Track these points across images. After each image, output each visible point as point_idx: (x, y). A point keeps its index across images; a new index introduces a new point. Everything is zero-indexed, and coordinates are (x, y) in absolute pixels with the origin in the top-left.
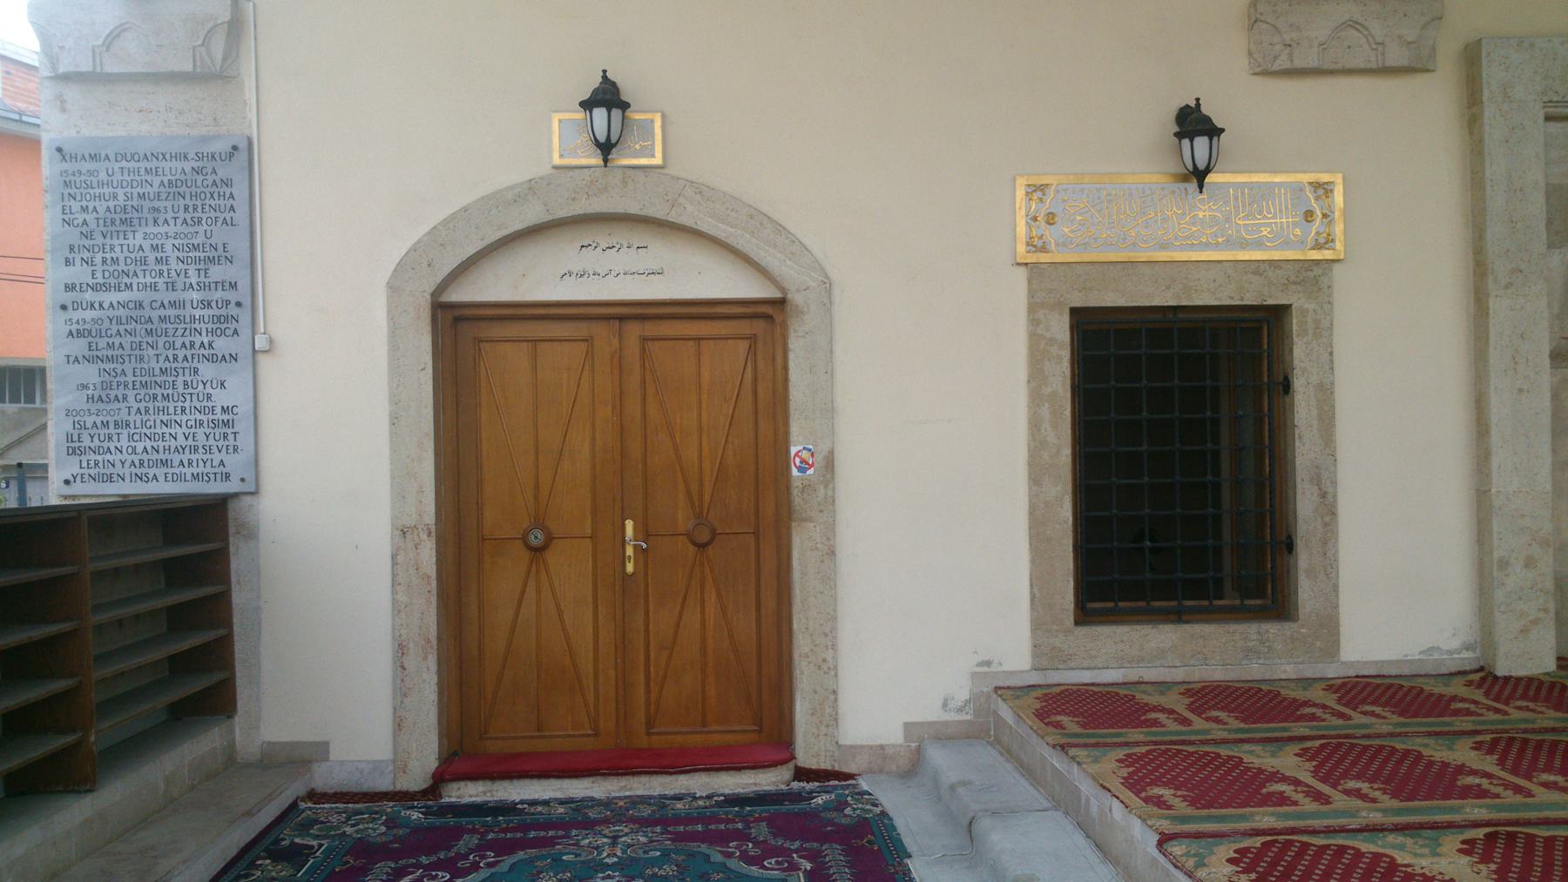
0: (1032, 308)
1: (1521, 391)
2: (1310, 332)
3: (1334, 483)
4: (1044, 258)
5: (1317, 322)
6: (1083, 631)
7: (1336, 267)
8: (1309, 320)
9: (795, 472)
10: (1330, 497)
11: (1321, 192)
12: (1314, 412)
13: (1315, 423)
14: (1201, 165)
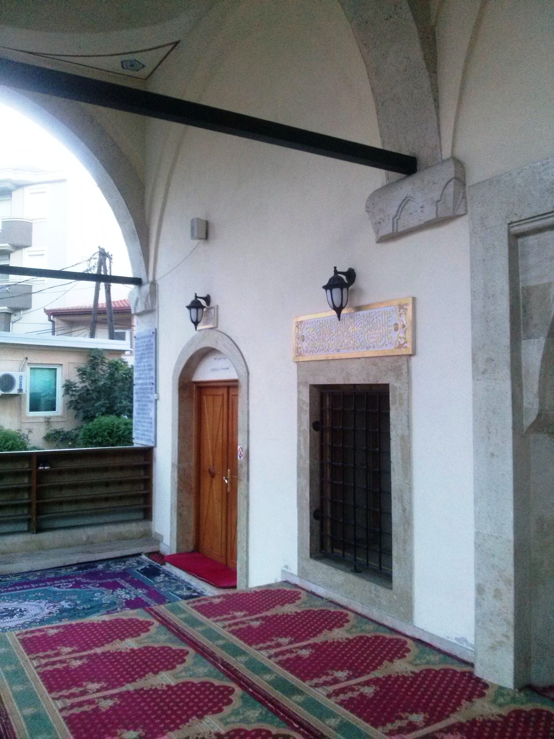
0: (299, 384)
1: (492, 455)
2: (398, 402)
3: (411, 503)
4: (301, 359)
5: (401, 395)
6: (312, 562)
7: (413, 359)
8: (397, 394)
9: (239, 458)
10: (407, 512)
11: (402, 310)
12: (400, 454)
13: (400, 461)
14: (338, 305)
